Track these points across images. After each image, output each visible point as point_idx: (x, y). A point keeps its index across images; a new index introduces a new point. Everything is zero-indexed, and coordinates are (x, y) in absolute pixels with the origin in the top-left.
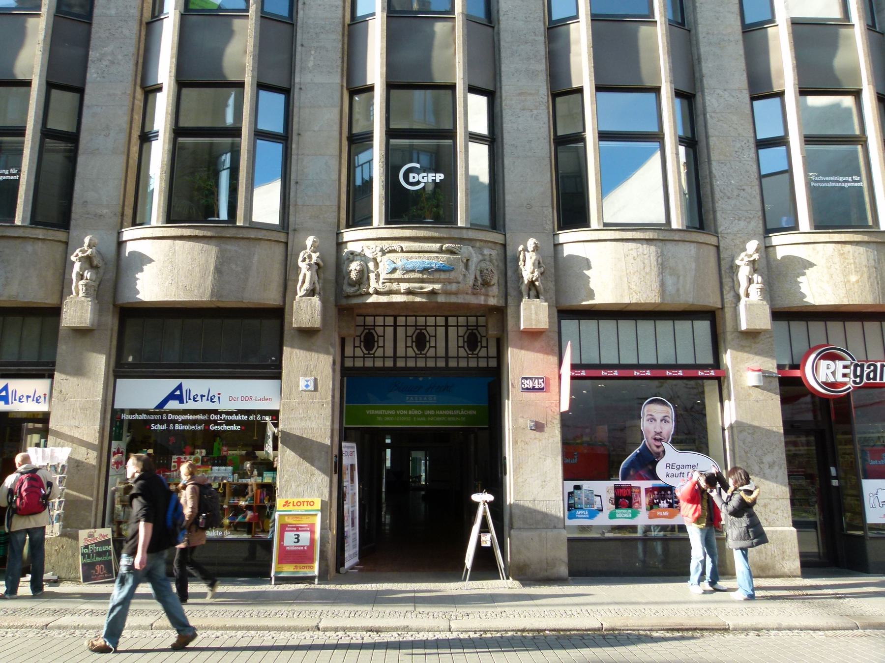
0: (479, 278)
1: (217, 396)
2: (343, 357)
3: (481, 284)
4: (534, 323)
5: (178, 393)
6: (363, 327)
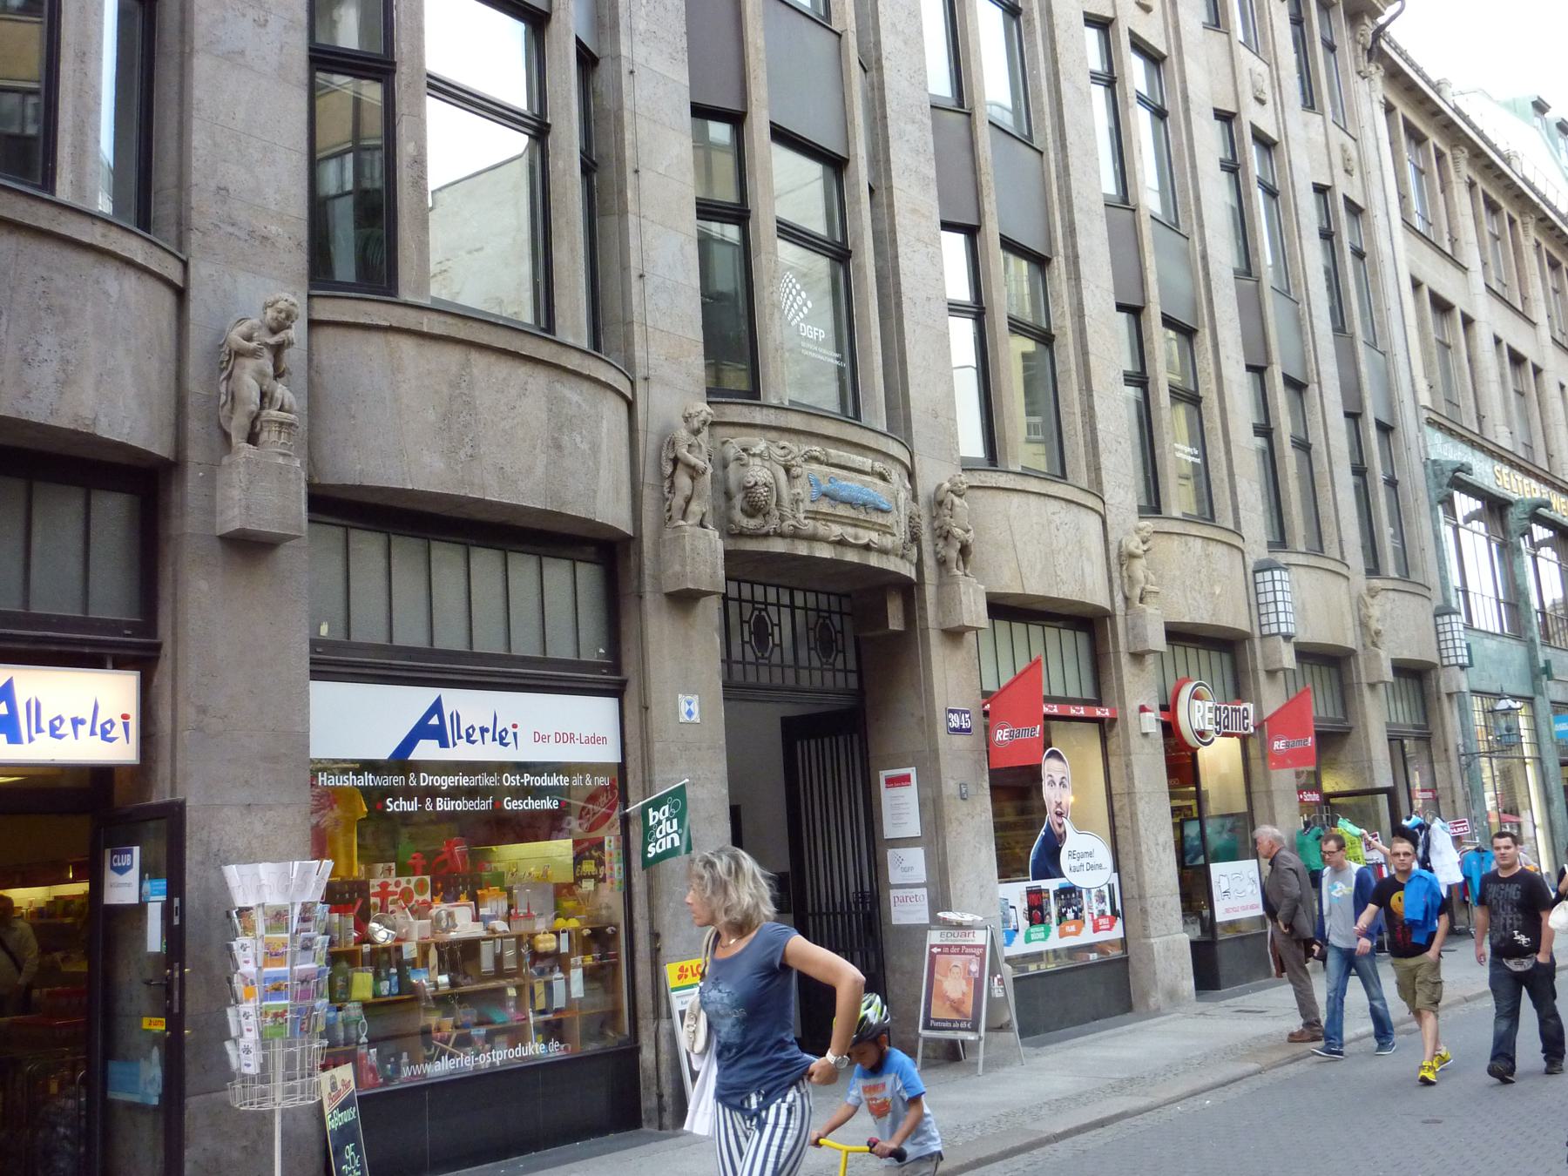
1: (511, 730)
5: (435, 721)
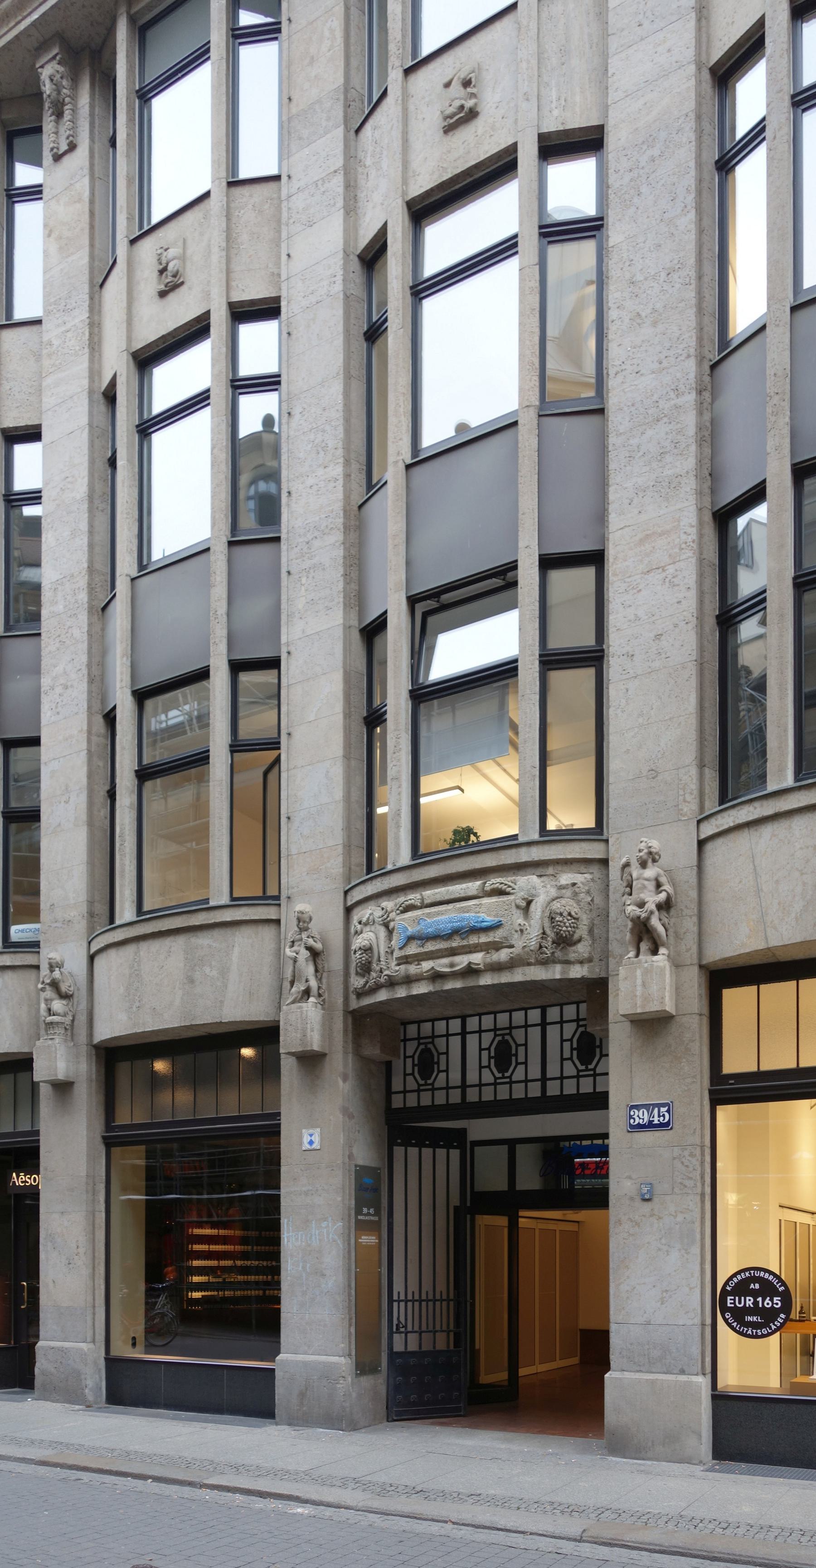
0: (548, 931)
2: (389, 1093)
3: (553, 942)
4: (639, 1003)
6: (416, 1042)
